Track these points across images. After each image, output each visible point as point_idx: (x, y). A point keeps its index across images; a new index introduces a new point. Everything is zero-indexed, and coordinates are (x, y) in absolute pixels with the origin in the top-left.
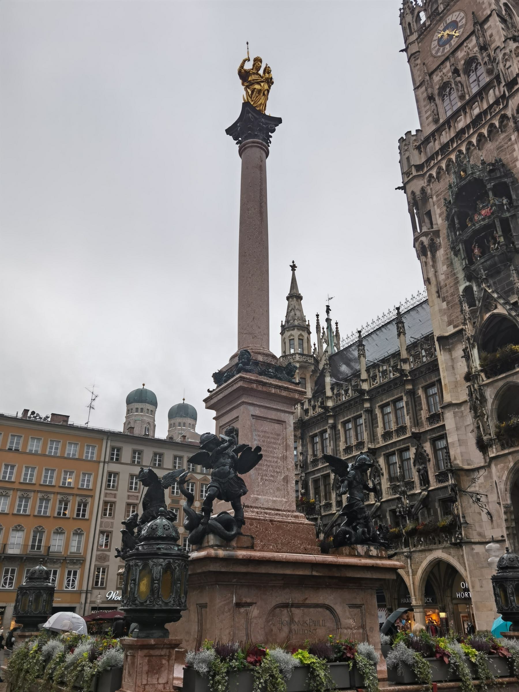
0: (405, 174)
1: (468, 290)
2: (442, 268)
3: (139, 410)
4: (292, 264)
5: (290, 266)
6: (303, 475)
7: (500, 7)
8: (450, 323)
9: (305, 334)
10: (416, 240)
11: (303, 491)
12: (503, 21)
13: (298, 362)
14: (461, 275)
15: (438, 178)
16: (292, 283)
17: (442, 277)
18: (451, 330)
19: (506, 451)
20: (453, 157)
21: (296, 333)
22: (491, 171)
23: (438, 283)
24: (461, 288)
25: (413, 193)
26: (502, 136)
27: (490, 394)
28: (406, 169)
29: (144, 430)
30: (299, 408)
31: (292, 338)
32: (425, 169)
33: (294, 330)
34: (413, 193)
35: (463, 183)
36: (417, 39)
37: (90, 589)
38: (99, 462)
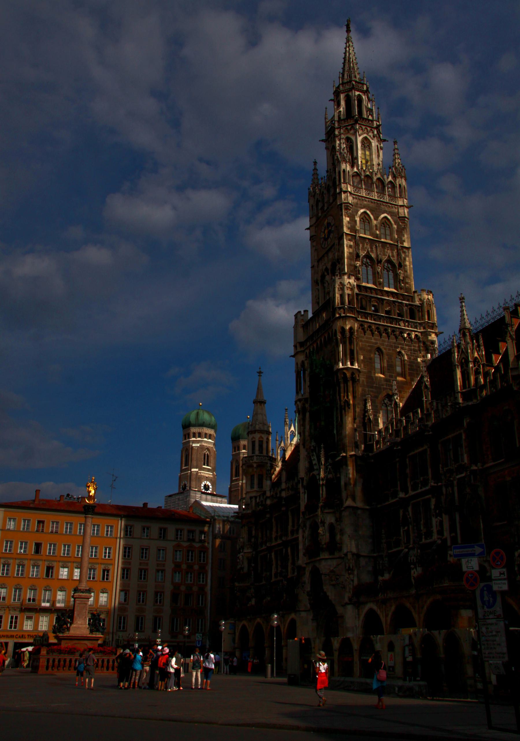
0: (295, 346)
3: (197, 435)
4: (259, 371)
5: (258, 372)
6: (254, 553)
7: (356, 221)
9: (264, 436)
10: (296, 402)
11: (253, 565)
13: (255, 462)
16: (258, 389)
19: (309, 561)
21: (257, 436)
27: (308, 524)
29: (203, 457)
30: (253, 500)
31: (254, 440)
33: (255, 433)
36: (315, 224)
37: (115, 631)
38: (116, 538)
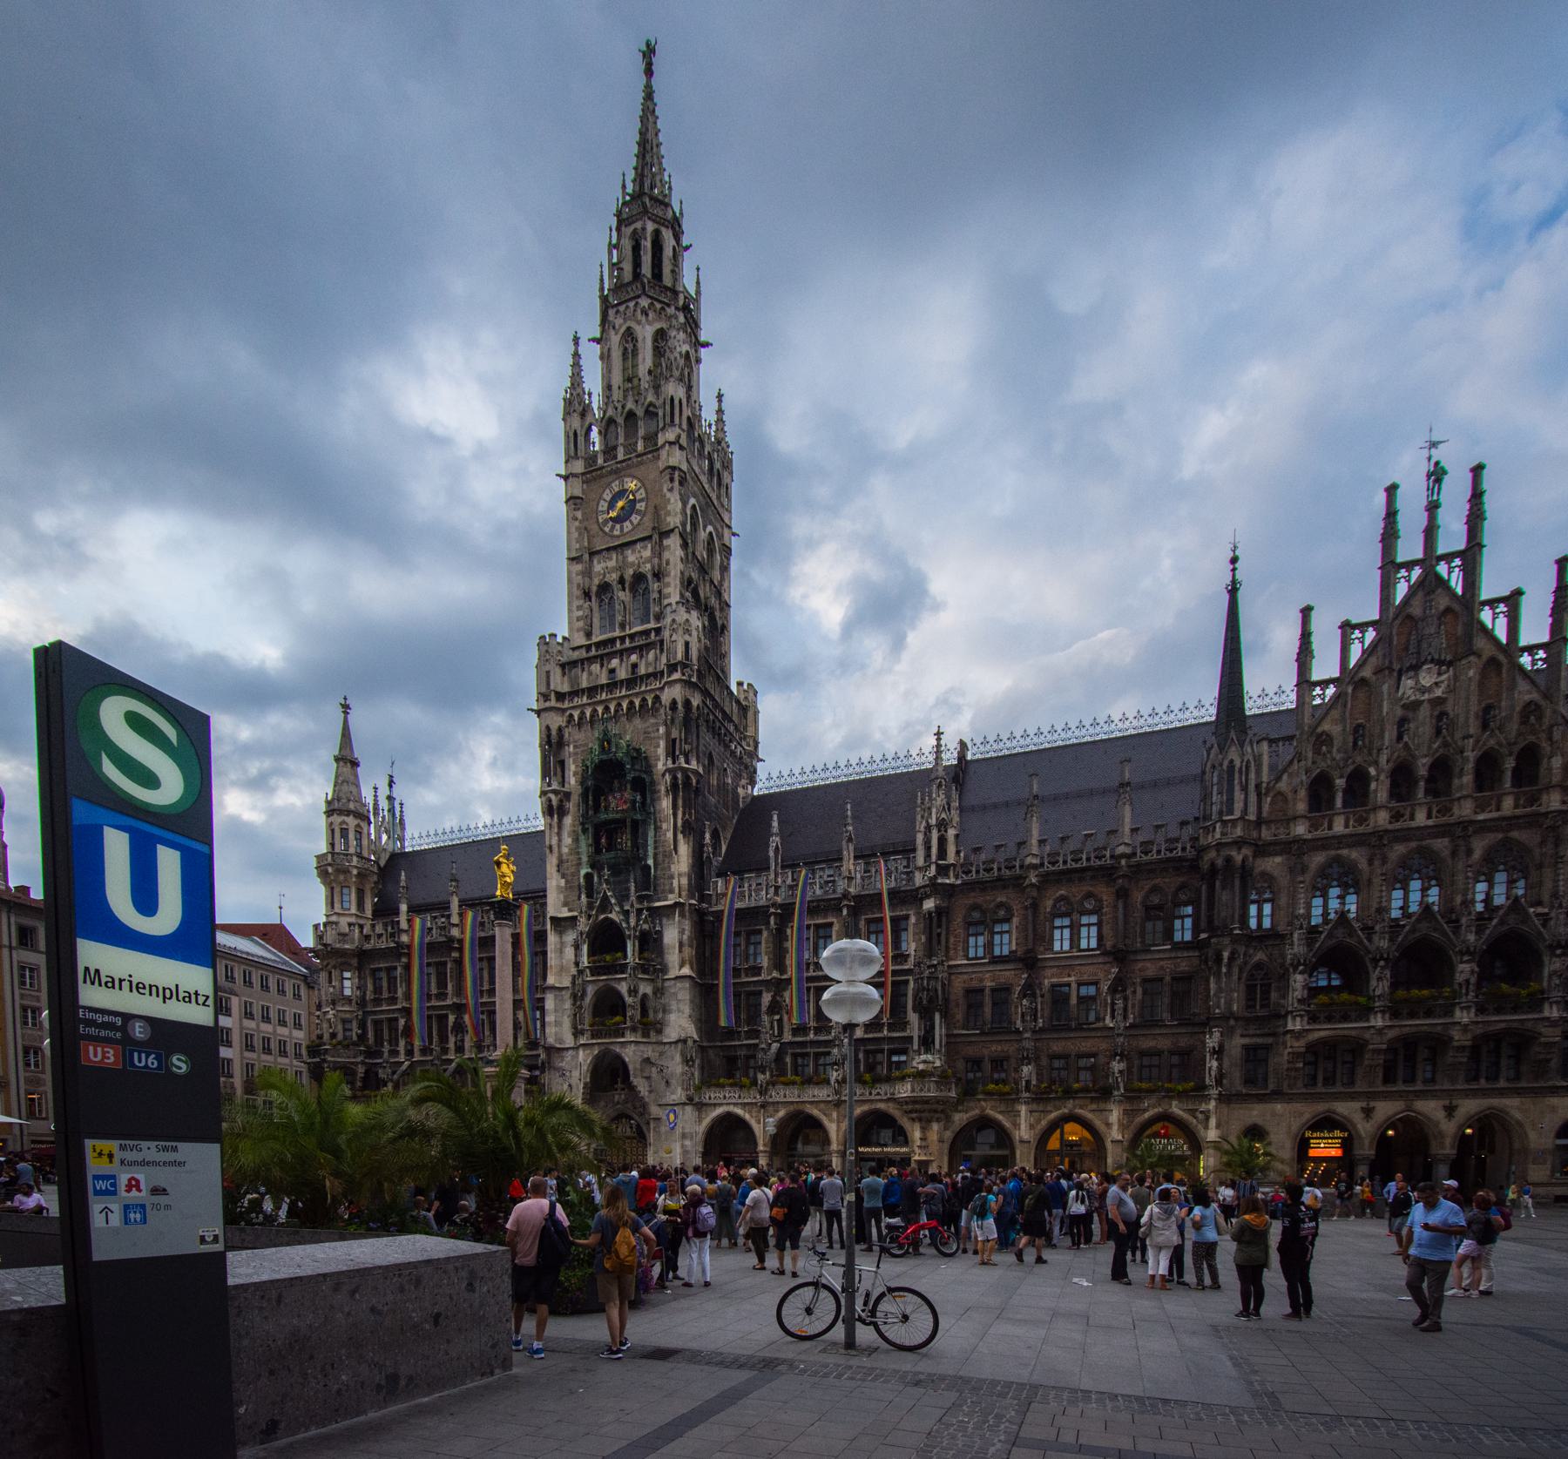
0: (544, 696)
1: (588, 877)
2: (567, 840)
8: (565, 904)
10: (543, 793)
12: (685, 545)
14: (585, 859)
15: (580, 725)
17: (565, 850)
18: (565, 913)
20: (600, 709)
22: (633, 758)
23: (560, 855)
24: (583, 872)
25: (548, 728)
26: (652, 721)
28: (544, 690)
32: (566, 705)
34: (548, 728)
35: (604, 757)
